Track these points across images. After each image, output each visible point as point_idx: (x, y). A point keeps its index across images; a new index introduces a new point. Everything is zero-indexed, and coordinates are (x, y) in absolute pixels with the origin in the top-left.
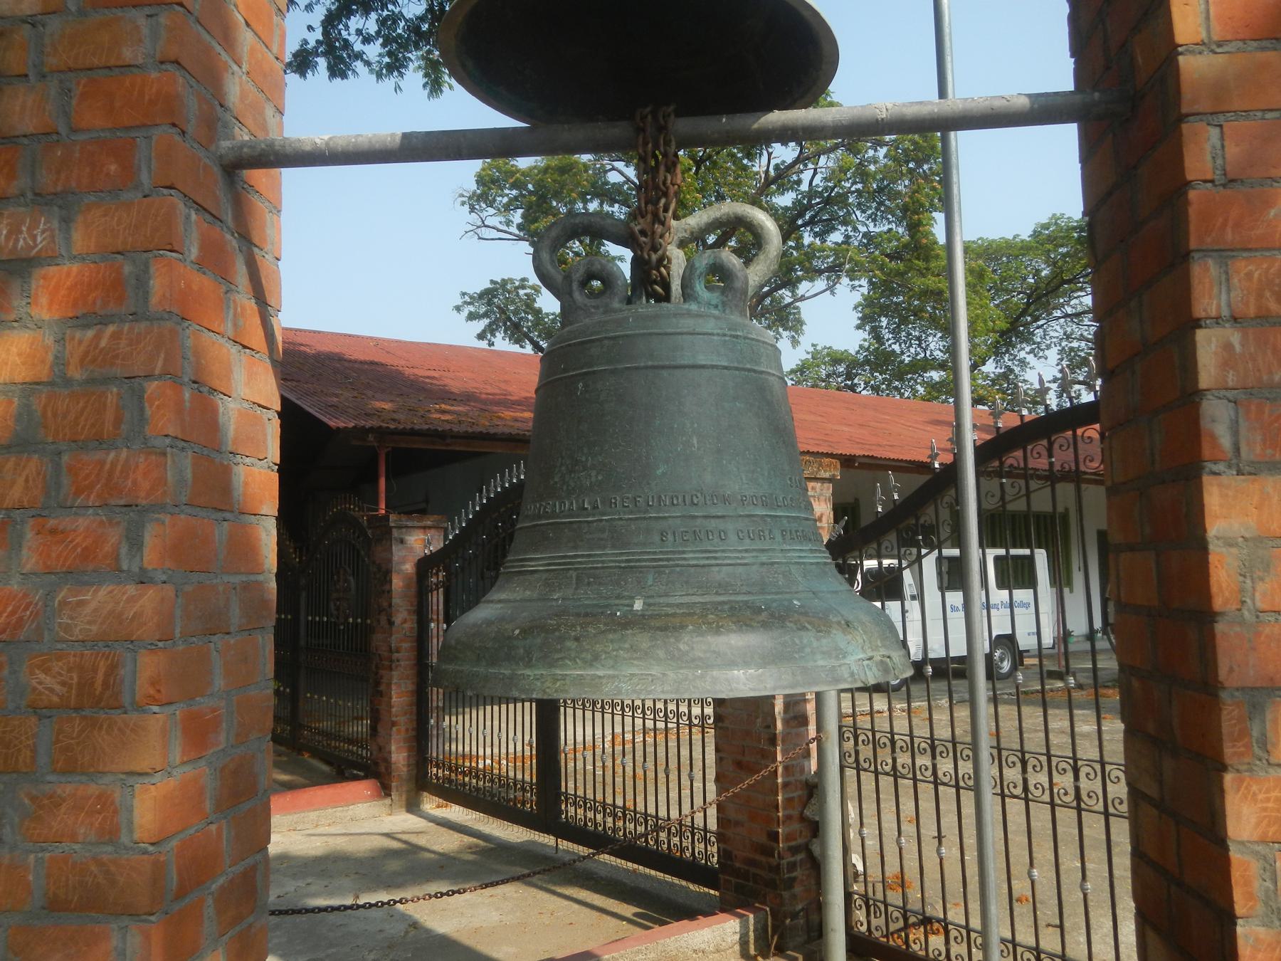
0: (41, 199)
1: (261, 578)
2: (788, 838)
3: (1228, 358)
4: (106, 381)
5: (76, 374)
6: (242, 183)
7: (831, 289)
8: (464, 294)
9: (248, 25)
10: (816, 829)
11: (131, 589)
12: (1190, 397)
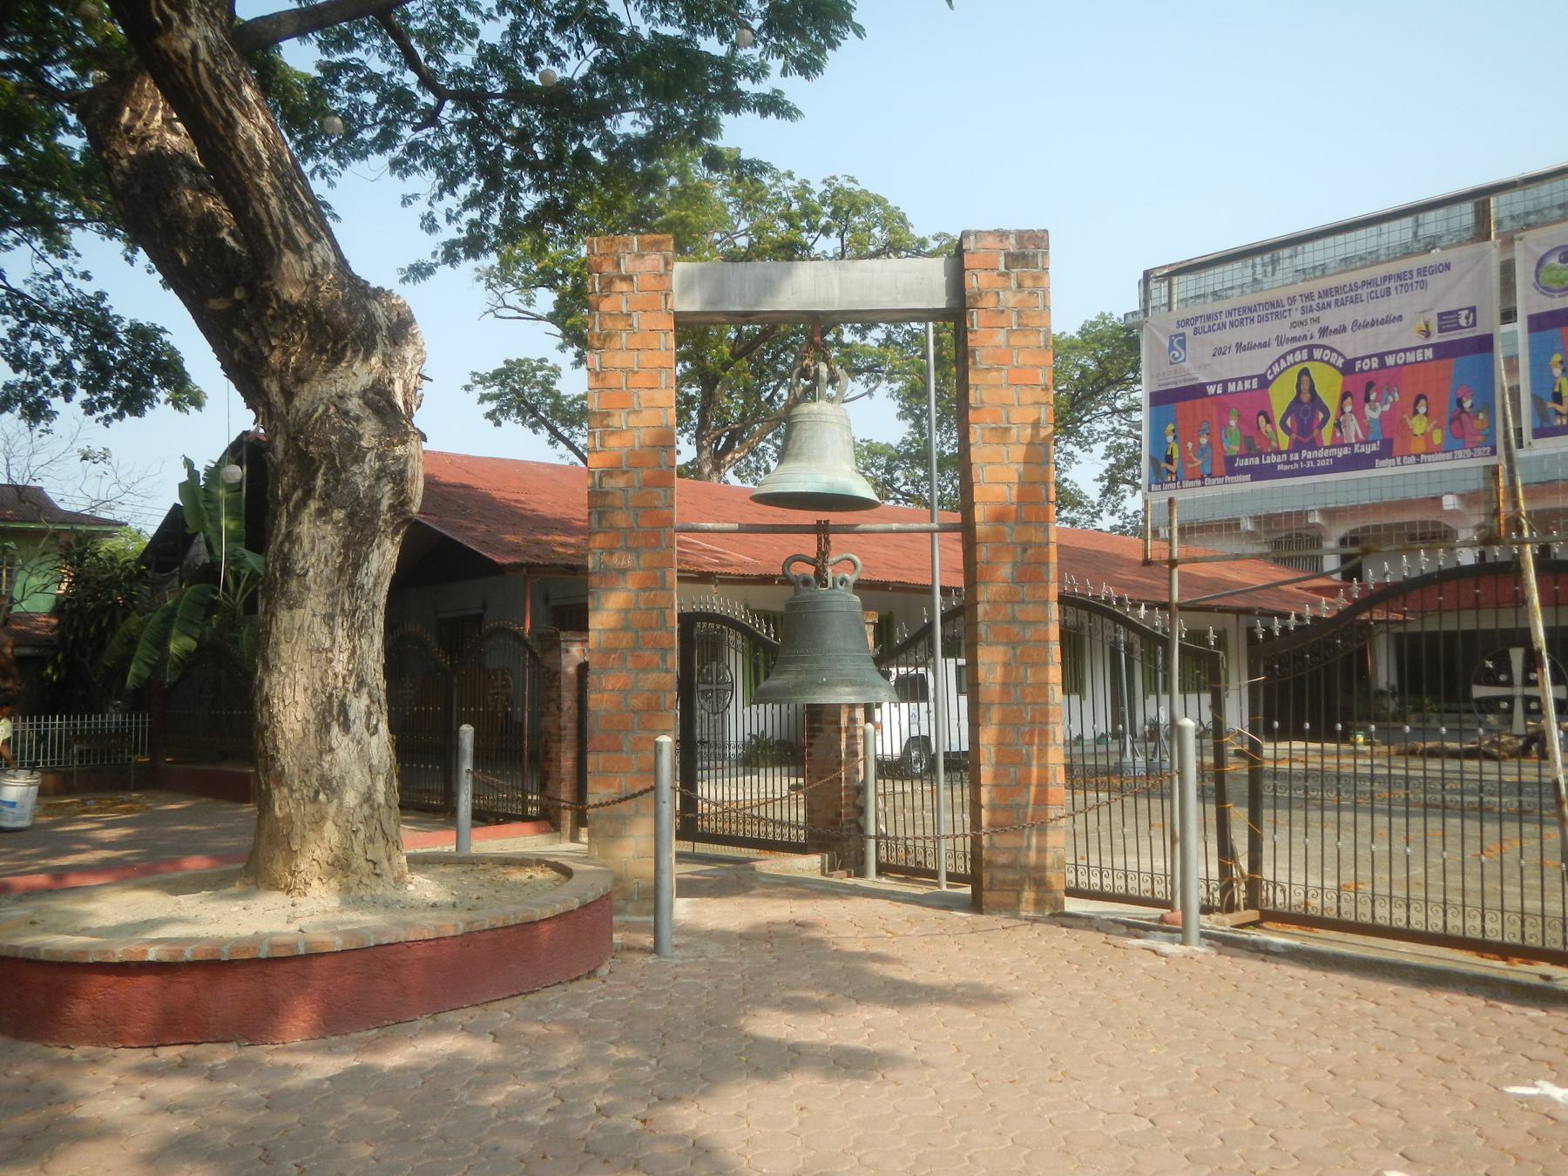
0: (628, 549)
2: (846, 815)
3: (986, 613)
4: (652, 609)
5: (643, 606)
7: (870, 393)
8: (474, 374)
10: (862, 811)
11: (663, 674)
12: (976, 623)
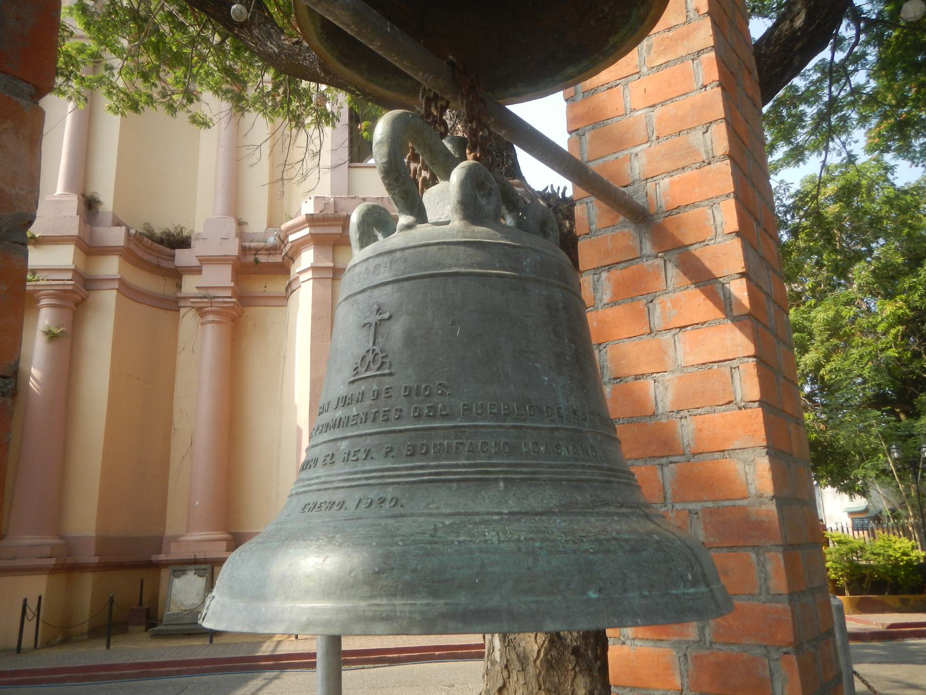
1: (744, 502)
6: (663, 215)
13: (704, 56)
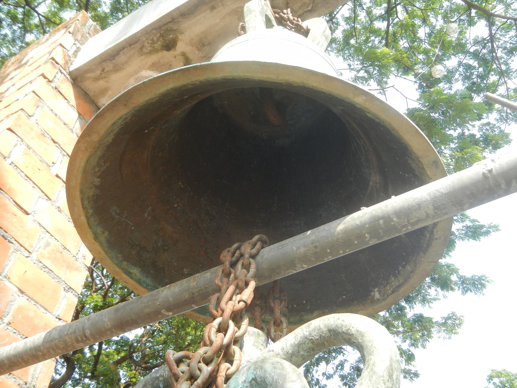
9: (22, 292)
13: (70, 295)
